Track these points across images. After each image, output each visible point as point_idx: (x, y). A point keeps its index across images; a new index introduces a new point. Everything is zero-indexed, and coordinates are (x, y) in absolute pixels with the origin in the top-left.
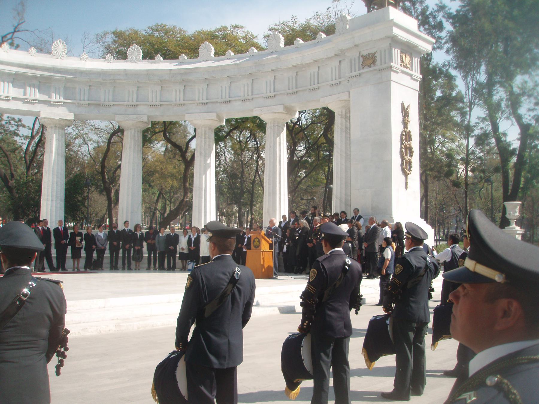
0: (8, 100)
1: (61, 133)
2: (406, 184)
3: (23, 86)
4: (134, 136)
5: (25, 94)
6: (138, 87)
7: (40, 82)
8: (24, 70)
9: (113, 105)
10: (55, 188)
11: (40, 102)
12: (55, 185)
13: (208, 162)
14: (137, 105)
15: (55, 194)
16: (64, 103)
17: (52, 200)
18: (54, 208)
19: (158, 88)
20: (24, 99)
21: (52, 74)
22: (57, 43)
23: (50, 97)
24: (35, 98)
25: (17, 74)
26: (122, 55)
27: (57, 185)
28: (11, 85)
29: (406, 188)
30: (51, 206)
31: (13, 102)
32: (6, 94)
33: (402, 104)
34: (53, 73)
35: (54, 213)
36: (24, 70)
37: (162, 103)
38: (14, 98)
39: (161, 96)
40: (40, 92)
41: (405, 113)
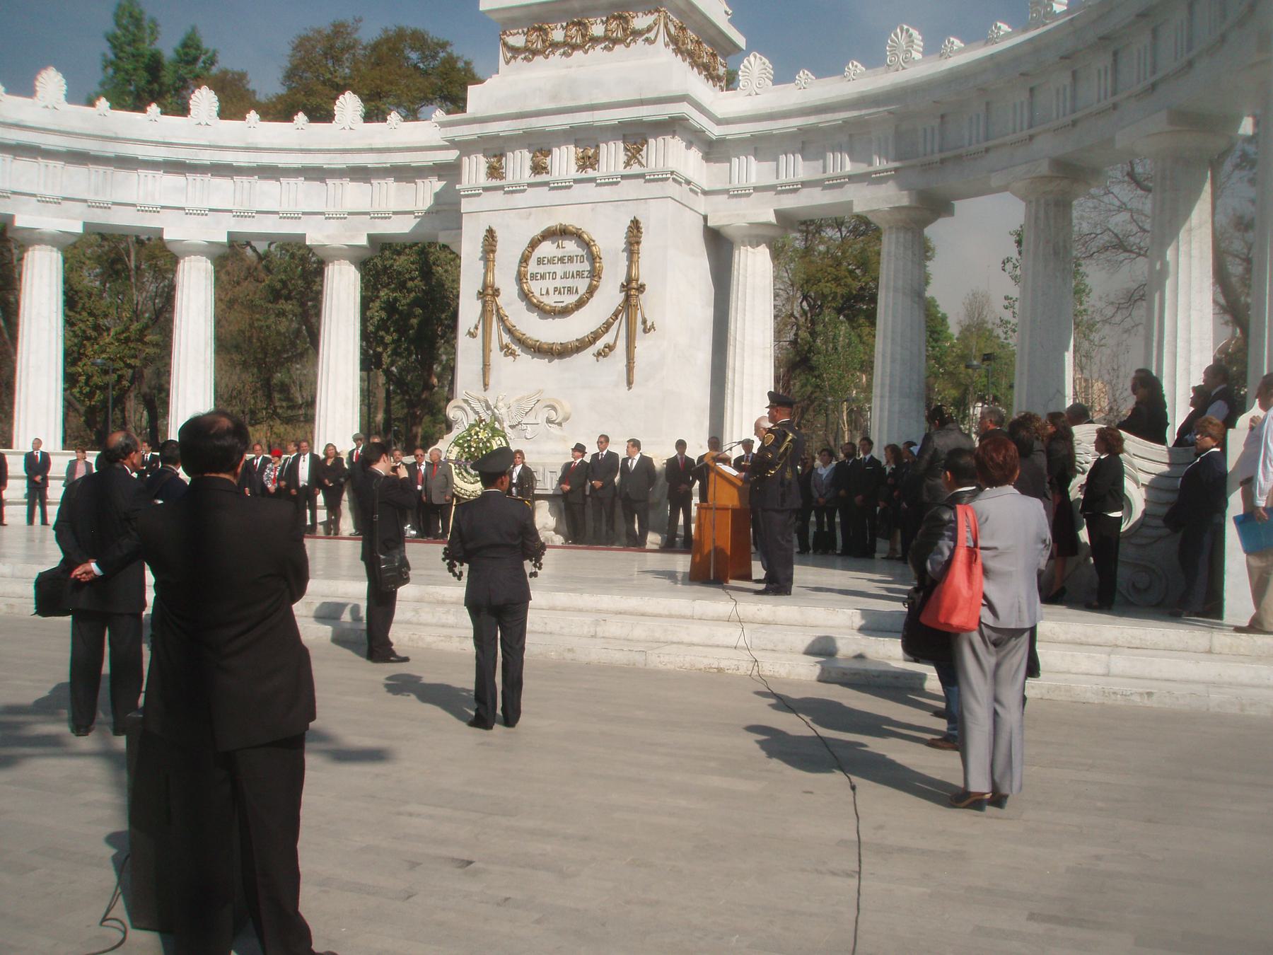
0: (795, 191)
1: (902, 240)
3: (821, 156)
4: (1037, 218)
5: (824, 172)
6: (1032, 90)
7: (851, 136)
8: (812, 120)
9: (987, 150)
10: (888, 370)
11: (853, 178)
12: (888, 360)
13: (1169, 254)
14: (1031, 138)
15: (887, 382)
16: (896, 170)
17: (882, 397)
18: (886, 413)
19: (1066, 79)
20: (823, 180)
21: (863, 112)
22: (896, 35)
23: (870, 164)
24: (843, 174)
25: (802, 131)
26: (321, 114)
27: (893, 361)
28: (799, 157)
30: (881, 410)
31: (805, 191)
32: (791, 178)
34: (866, 108)
35: (885, 426)
36: (812, 120)
37: (1074, 117)
38: (805, 184)
39: (1074, 98)
40: (852, 159)
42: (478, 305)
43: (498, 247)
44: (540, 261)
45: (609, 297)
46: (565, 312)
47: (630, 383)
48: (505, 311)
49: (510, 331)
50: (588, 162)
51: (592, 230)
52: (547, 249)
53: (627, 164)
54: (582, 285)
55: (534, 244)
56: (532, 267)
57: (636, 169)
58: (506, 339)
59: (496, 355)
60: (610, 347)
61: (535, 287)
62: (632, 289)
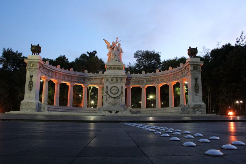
2: (197, 94)
29: (197, 96)
33: (195, 78)
41: (196, 80)
42: (106, 93)
43: (108, 87)
44: (112, 89)
45: (120, 93)
46: (114, 94)
47: (122, 101)
48: (109, 94)
49: (109, 96)
50: (117, 80)
51: (117, 86)
52: (113, 88)
53: (121, 81)
54: (117, 92)
55: (111, 88)
56: (111, 90)
57: (122, 82)
58: (109, 96)
59: (108, 98)
60: (120, 98)
61: (112, 92)
62: (122, 92)
